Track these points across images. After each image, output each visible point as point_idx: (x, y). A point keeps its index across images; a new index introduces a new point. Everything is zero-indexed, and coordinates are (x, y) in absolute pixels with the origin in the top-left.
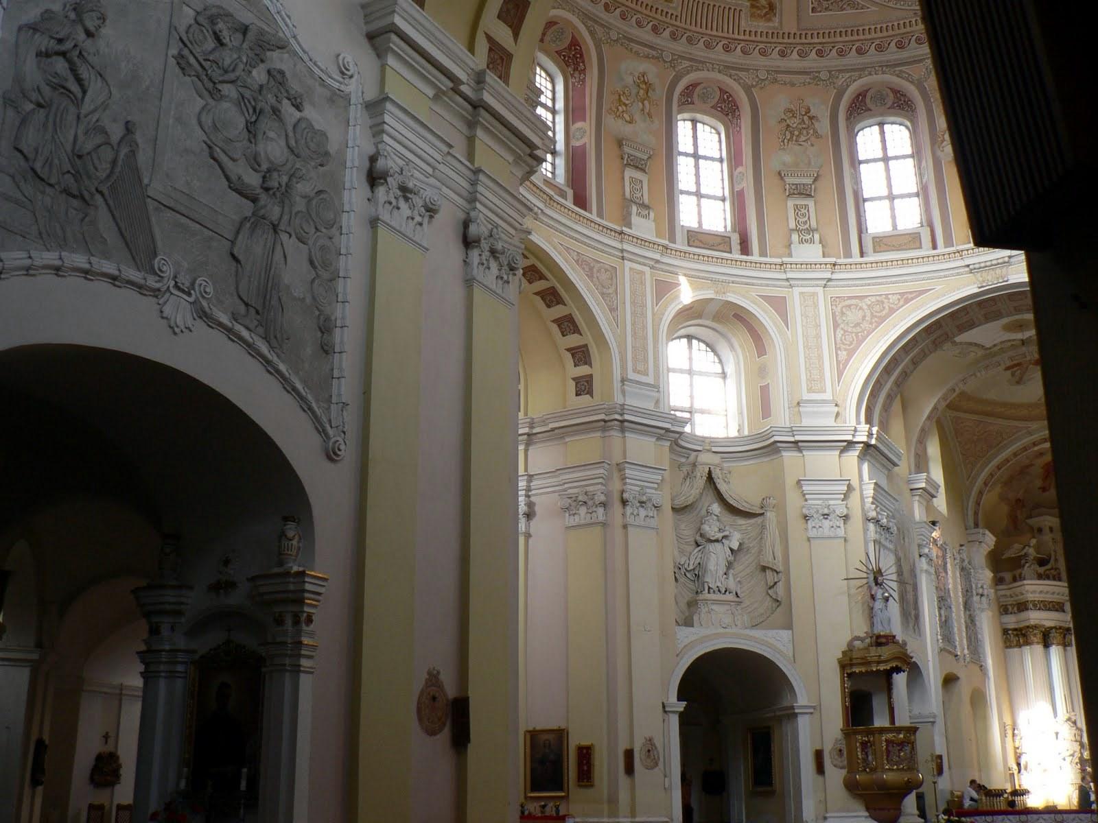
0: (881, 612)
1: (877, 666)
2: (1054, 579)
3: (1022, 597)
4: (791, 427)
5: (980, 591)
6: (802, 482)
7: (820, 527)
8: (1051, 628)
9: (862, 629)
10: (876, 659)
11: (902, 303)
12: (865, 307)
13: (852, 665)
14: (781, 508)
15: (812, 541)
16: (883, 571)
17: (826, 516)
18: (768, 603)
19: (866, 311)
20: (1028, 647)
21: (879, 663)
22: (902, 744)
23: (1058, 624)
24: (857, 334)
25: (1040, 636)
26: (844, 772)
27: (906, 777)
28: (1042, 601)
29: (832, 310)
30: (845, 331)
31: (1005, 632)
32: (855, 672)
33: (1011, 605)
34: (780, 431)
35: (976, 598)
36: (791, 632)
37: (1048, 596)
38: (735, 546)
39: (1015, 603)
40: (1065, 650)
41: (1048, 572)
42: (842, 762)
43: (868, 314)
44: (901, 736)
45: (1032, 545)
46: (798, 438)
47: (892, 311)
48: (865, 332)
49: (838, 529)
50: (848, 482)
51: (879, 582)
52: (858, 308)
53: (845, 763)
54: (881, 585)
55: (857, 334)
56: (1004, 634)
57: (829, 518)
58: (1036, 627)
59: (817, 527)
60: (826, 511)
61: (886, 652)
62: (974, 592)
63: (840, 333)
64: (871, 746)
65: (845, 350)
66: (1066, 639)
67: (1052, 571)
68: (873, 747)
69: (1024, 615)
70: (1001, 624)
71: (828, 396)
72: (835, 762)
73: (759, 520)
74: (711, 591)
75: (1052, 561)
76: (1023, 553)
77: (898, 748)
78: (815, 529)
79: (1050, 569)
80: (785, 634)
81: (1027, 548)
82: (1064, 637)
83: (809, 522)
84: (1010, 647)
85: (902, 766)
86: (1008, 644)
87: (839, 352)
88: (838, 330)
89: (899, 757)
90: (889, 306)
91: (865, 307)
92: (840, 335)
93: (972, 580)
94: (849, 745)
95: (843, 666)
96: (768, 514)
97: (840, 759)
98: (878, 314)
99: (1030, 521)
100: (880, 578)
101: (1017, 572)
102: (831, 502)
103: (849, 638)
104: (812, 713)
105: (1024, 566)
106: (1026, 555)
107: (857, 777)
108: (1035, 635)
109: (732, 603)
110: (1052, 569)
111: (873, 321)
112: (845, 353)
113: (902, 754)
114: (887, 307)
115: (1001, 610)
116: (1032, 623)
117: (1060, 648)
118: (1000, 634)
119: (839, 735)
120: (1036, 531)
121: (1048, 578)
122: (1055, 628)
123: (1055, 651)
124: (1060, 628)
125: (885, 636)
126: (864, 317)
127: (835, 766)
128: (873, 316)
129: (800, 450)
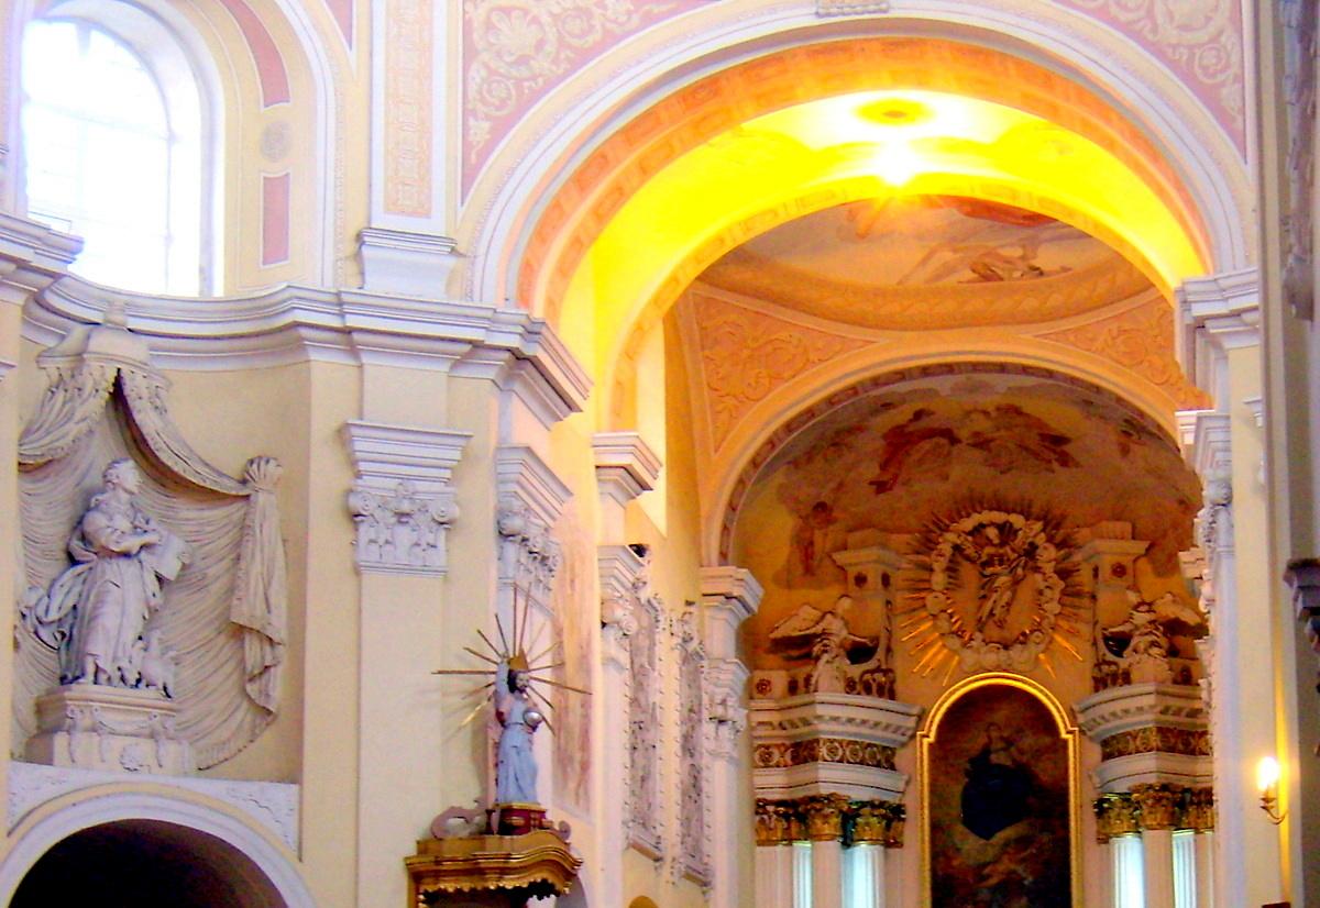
0: (518, 753)
1: (500, 879)
2: (881, 694)
3: (805, 730)
4: (338, 294)
5: (720, 711)
6: (355, 431)
7: (387, 542)
8: (863, 804)
9: (466, 794)
10: (500, 863)
11: (636, 20)
12: (546, 19)
13: (437, 875)
14: (296, 490)
15: (371, 580)
16: (529, 660)
17: (402, 517)
18: (244, 715)
19: (547, 29)
20: (808, 844)
21: (503, 871)
23: (877, 796)
24: (519, 82)
25: (835, 820)
28: (850, 743)
29: (464, 12)
30: (491, 72)
31: (760, 806)
32: (445, 890)
33: (777, 746)
34: (309, 300)
35: (708, 728)
36: (295, 788)
37: (865, 730)
38: (170, 570)
39: (787, 743)
40: (886, 856)
41: (868, 676)
43: (552, 36)
45: (840, 611)
46: (352, 321)
47: (610, 39)
48: (540, 81)
49: (431, 551)
50: (462, 442)
51: (520, 684)
52: (529, 18)
54: (522, 691)
55: (519, 82)
56: (757, 813)
57: (411, 521)
58: (830, 799)
59: (381, 541)
60: (406, 507)
61: (521, 848)
62: (706, 715)
63: (477, 74)
65: (487, 117)
66: (891, 833)
67: (877, 676)
69: (804, 773)
70: (752, 788)
71: (435, 225)
73: (235, 511)
74: (102, 677)
75: (880, 653)
76: (818, 629)
78: (374, 547)
79: (872, 672)
80: (283, 794)
81: (829, 616)
82: (888, 827)
83: (363, 528)
86: (764, 835)
87: (472, 122)
88: (475, 66)
90: (603, 26)
91: (546, 19)
92: (478, 80)
93: (703, 683)
95: (416, 877)
96: (261, 499)
98: (576, 42)
99: (840, 557)
100: (521, 676)
102: (421, 486)
103: (439, 811)
105: (818, 658)
106: (824, 634)
109: (156, 712)
110: (878, 669)
111: (562, 56)
112: (486, 125)
114: (598, 27)
115: (757, 756)
116: (824, 790)
117: (879, 848)
118: (748, 809)
120: (851, 580)
121: (868, 690)
122: (871, 804)
124: (882, 804)
125: (525, 813)
126: (540, 45)
128: (562, 44)
129: (353, 351)
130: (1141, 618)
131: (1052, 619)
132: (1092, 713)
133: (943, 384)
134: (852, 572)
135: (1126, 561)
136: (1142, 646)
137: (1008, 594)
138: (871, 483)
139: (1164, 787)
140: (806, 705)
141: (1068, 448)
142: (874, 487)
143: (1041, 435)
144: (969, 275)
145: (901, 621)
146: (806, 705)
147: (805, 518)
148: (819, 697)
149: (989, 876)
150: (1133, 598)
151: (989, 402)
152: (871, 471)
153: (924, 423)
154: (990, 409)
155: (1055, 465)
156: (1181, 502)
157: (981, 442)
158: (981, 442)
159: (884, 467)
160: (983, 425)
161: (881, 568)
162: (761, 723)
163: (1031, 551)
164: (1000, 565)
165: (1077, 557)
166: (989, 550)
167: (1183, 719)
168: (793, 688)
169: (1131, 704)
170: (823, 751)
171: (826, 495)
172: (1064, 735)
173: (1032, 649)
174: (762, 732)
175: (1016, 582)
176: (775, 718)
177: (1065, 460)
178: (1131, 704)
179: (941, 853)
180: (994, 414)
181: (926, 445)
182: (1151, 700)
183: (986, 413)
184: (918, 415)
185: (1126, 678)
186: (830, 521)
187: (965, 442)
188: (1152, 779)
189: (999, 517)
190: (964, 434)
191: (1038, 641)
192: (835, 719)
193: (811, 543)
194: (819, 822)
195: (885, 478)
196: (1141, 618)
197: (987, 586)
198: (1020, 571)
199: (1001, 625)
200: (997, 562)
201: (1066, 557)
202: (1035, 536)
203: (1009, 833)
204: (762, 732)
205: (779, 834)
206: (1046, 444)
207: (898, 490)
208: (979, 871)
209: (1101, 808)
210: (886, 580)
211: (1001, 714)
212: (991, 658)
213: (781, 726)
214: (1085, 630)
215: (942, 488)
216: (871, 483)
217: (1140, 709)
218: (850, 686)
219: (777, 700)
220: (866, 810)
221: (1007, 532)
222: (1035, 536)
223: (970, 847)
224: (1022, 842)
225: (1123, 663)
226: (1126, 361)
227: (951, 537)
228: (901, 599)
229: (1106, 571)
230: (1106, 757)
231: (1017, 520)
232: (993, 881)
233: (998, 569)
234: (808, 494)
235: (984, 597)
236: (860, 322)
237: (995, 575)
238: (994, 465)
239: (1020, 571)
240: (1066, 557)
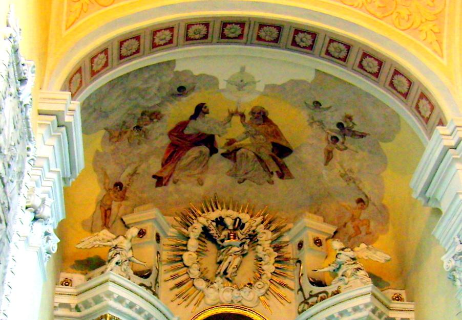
75: (153, 276)
131: (270, 275)
135: (322, 237)
136: (349, 272)
137: (238, 260)
138: (154, 177)
140: (101, 284)
141: (288, 161)
142: (155, 180)
143: (274, 144)
146: (101, 284)
152: (155, 165)
154: (247, 111)
155: (275, 177)
159: (164, 164)
160: (236, 130)
162: (62, 305)
163: (253, 237)
164: (234, 238)
165: (286, 238)
169: (348, 306)
171: (123, 179)
174: (60, 312)
177: (283, 173)
180: (248, 118)
181: (194, 152)
182: (368, 299)
183: (243, 116)
184: (200, 110)
186: (123, 198)
187: (221, 151)
189: (235, 214)
190: (221, 142)
191: (259, 287)
193: (110, 209)
195: (164, 174)
198: (246, 247)
200: (232, 237)
201: (279, 237)
202: (257, 226)
206: (274, 154)
207: (171, 187)
213: (77, 309)
215: (201, 191)
216: (154, 177)
217: (356, 309)
222: (257, 226)
226: (378, 14)
227: (202, 220)
233: (232, 241)
234: (115, 172)
235: (220, 263)
237: (231, 246)
238: (235, 175)
239: (246, 247)
240: (279, 237)
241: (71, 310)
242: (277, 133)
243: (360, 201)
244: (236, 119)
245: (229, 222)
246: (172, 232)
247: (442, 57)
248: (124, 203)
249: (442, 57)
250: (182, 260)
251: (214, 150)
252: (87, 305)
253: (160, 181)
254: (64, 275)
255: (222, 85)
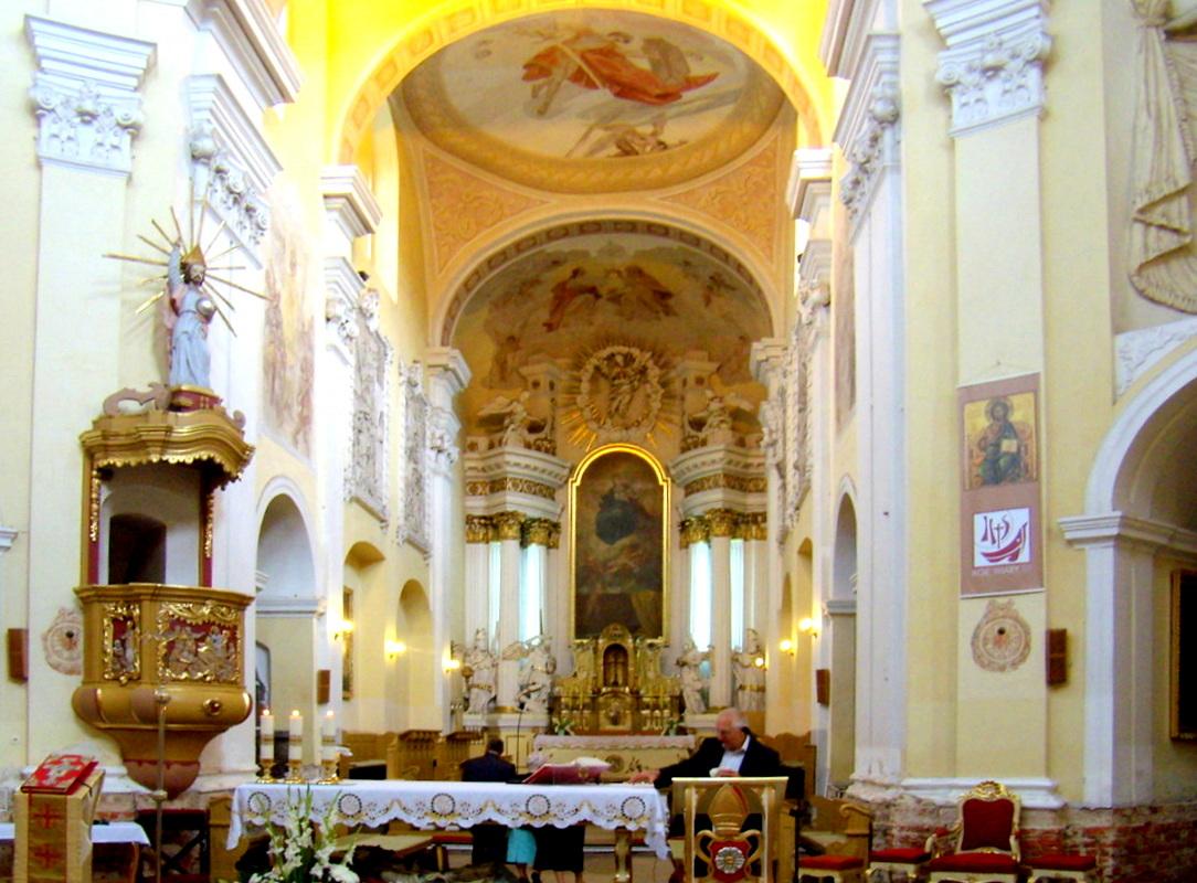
2: (547, 451)
3: (498, 471)
5: (438, 443)
8: (534, 520)
20: (499, 543)
22: (204, 629)
23: (544, 516)
25: (516, 528)
26: (76, 681)
27: (208, 696)
28: (526, 482)
31: (469, 520)
33: (481, 483)
35: (429, 455)
37: (536, 474)
39: (487, 481)
40: (548, 554)
41: (539, 442)
42: (71, 659)
44: (206, 611)
45: (522, 399)
53: (81, 661)
56: (467, 523)
58: (513, 515)
62: (428, 443)
64: (134, 627)
66: (552, 540)
67: (545, 443)
68: (138, 630)
69: (497, 498)
72: (55, 659)
75: (547, 429)
76: (508, 410)
77: (198, 636)
79: (542, 440)
81: (515, 404)
82: (550, 535)
84: (474, 541)
85: (200, 675)
86: (471, 538)
89: (196, 654)
93: (427, 423)
94: (88, 624)
97: (66, 654)
99: (524, 371)
101: (497, 436)
104: (8, 548)
105: (507, 427)
106: (511, 414)
107: (99, 692)
108: (510, 527)
110: (546, 439)
113: (203, 649)
115: (468, 489)
116: (510, 509)
117: (543, 548)
118: (461, 523)
119: (69, 602)
120: (530, 384)
121: (538, 449)
122: (539, 520)
123: (535, 551)
124: (546, 521)
127: (56, 667)
130: (715, 406)
132: (682, 467)
133: (593, 244)
134: (531, 380)
135: (705, 375)
136: (715, 424)
137: (628, 397)
139: (727, 511)
141: (671, 302)
144: (614, 150)
145: (561, 412)
147: (502, 345)
148: (508, 449)
149: (611, 567)
150: (709, 394)
151: (620, 263)
153: (580, 281)
154: (622, 269)
155: (662, 315)
156: (741, 338)
157: (615, 298)
158: (615, 298)
159: (553, 313)
160: (616, 283)
161: (549, 379)
163: (643, 371)
165: (673, 374)
166: (617, 370)
167: (739, 469)
168: (491, 446)
169: (708, 458)
170: (509, 485)
171: (516, 332)
172: (661, 482)
173: (643, 430)
174: (469, 473)
175: (634, 390)
176: (480, 465)
178: (708, 458)
179: (582, 552)
180: (625, 274)
181: (580, 299)
182: (721, 455)
183: (619, 272)
184: (576, 273)
185: (704, 443)
186: (517, 348)
187: (605, 296)
188: (719, 506)
189: (625, 350)
190: (603, 291)
192: (517, 465)
193: (505, 362)
194: (506, 529)
196: (715, 406)
197: (615, 390)
198: (636, 383)
199: (623, 416)
203: (625, 541)
204: (469, 473)
205: (481, 537)
207: (562, 330)
208: (605, 565)
209: (684, 527)
210: (552, 386)
211: (623, 468)
212: (617, 435)
214: (676, 419)
215: (592, 329)
217: (713, 462)
218: (528, 446)
219: (480, 453)
220: (536, 524)
221: (629, 359)
223: (601, 549)
224: (634, 547)
225: (702, 435)
227: (594, 361)
228: (561, 398)
229: (691, 382)
230: (687, 495)
231: (635, 352)
232: (615, 569)
233: (622, 380)
234: (505, 329)
235: (613, 399)
236: (538, 185)
237: (622, 385)
239: (636, 383)
241: (478, 471)
242: (656, 283)
243: (741, 338)
244: (614, 276)
245: (619, 359)
246: (564, 377)
247: (772, 262)
248: (518, 353)
249: (772, 262)
250: (575, 403)
251: (598, 296)
252: (490, 468)
253: (550, 327)
254: (470, 439)
255: (593, 254)
